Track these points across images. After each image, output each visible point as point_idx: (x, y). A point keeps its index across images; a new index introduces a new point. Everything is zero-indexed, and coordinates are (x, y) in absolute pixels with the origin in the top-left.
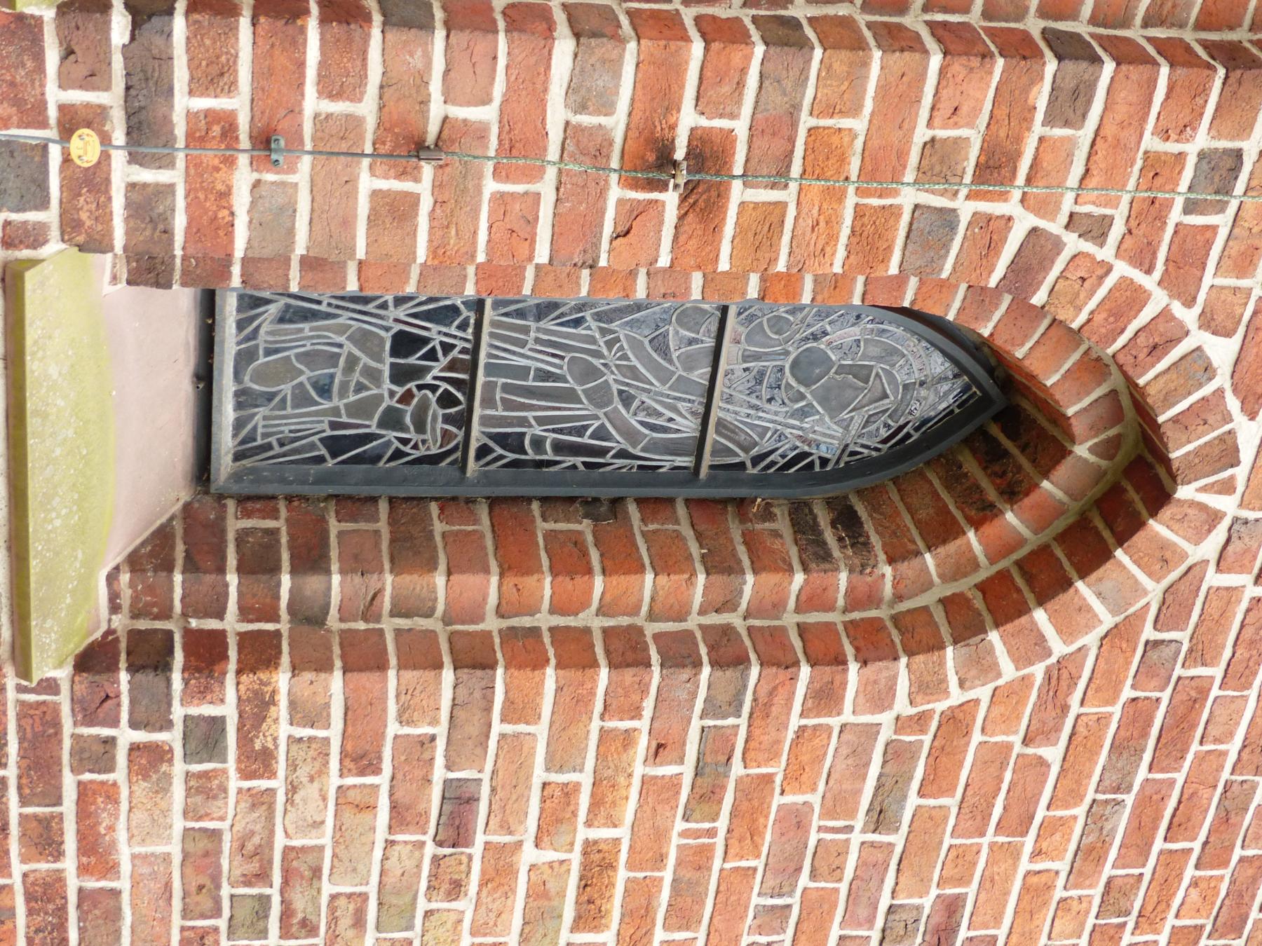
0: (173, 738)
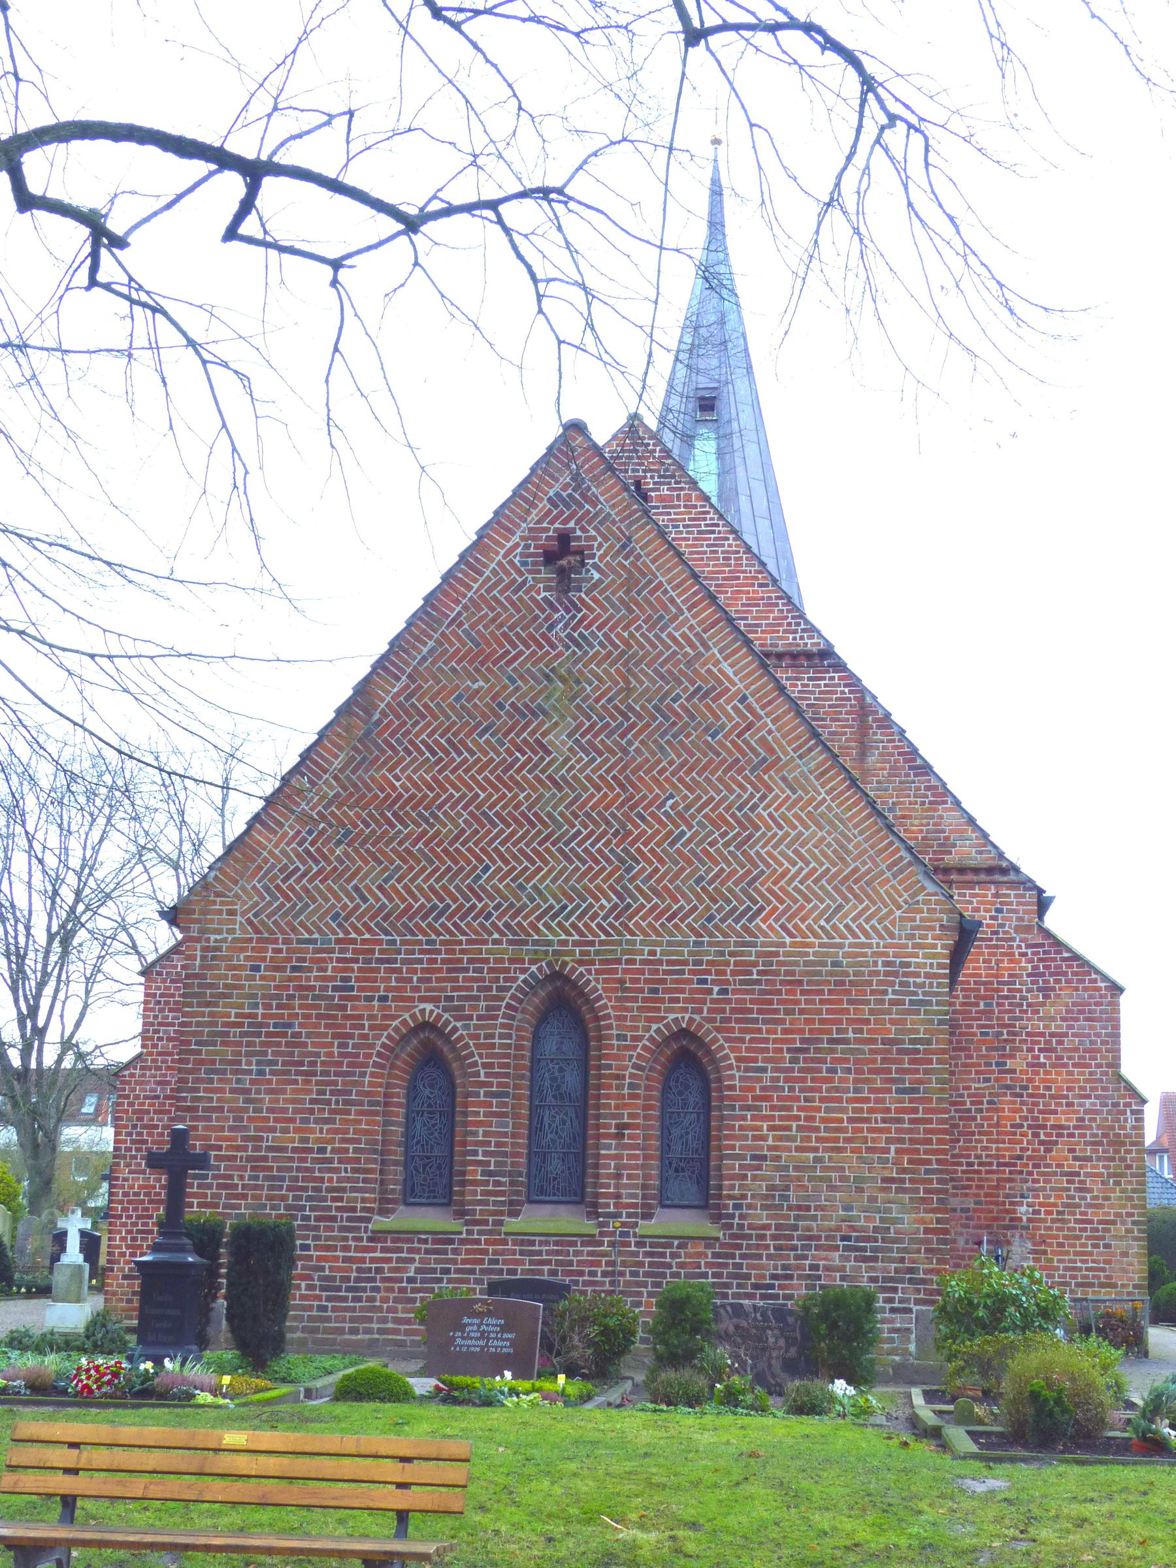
0: (737, 1213)
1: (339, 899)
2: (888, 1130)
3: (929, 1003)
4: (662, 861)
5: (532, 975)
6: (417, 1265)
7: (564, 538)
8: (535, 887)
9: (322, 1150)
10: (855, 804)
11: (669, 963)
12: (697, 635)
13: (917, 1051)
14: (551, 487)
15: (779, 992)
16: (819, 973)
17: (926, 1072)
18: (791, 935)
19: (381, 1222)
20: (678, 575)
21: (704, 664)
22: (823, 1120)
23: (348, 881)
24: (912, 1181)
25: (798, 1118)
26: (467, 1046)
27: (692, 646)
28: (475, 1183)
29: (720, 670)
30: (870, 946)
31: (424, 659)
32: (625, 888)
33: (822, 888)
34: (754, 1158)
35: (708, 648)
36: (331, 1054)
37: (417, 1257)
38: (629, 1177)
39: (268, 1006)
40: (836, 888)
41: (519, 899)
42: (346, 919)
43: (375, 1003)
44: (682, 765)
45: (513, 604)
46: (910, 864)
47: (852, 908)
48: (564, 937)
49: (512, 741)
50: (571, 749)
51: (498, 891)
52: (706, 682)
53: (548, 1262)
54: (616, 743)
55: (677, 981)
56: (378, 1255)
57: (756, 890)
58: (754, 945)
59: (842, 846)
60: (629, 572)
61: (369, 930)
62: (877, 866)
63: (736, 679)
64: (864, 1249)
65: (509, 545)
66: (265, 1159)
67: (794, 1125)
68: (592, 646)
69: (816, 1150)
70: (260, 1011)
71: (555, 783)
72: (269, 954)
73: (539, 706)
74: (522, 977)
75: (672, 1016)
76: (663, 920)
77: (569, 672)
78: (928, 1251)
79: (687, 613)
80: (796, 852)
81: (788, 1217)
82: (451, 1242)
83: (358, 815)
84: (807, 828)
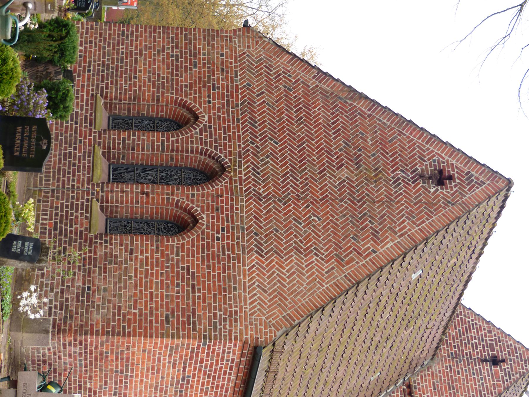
0: (103, 241)
1: (257, 86)
2: (146, 309)
3: (215, 331)
4: (285, 214)
5: (223, 160)
6: (80, 112)
7: (451, 178)
8: (268, 162)
9: (135, 78)
10: (322, 300)
11: (232, 216)
12: (406, 232)
13: (189, 324)
14: (477, 172)
15: (219, 263)
16: (229, 281)
17: (178, 328)
18: (249, 270)
19: (101, 102)
20: (437, 225)
21: (391, 235)
22: (151, 281)
23: (267, 90)
24: (119, 320)
25: (152, 269)
26: (187, 133)
27: (400, 230)
28: (119, 134)
29: (388, 242)
30: (245, 304)
31: (380, 120)
32: (270, 199)
33: (275, 284)
34: (132, 250)
35: (400, 236)
36: (182, 81)
37: (84, 112)
38: (122, 197)
39: (204, 59)
40: (275, 290)
41: (262, 155)
42: (248, 89)
43: (207, 99)
44: (336, 224)
45: (413, 156)
46: (291, 324)
47: (266, 298)
48: (243, 173)
49: (342, 155)
50: (340, 178)
51: (265, 147)
52: (382, 235)
53: (79, 162)
54: (345, 197)
55: (223, 218)
56: (85, 97)
57: (273, 255)
58: (243, 253)
59: (299, 293)
60: (435, 204)
61: (243, 97)
62: (289, 309)
63: (385, 248)
64: (83, 296)
65: (443, 155)
66: (131, 57)
67: (149, 268)
68: (395, 188)
69: (136, 276)
70: (202, 56)
71: (322, 171)
72: (229, 60)
73: (361, 166)
74: (222, 156)
75: (205, 216)
76: (254, 214)
77: (380, 178)
78: (82, 325)
79: (417, 228)
80: (294, 273)
81: (100, 263)
82: (91, 125)
83: (299, 94)
84: (308, 278)
